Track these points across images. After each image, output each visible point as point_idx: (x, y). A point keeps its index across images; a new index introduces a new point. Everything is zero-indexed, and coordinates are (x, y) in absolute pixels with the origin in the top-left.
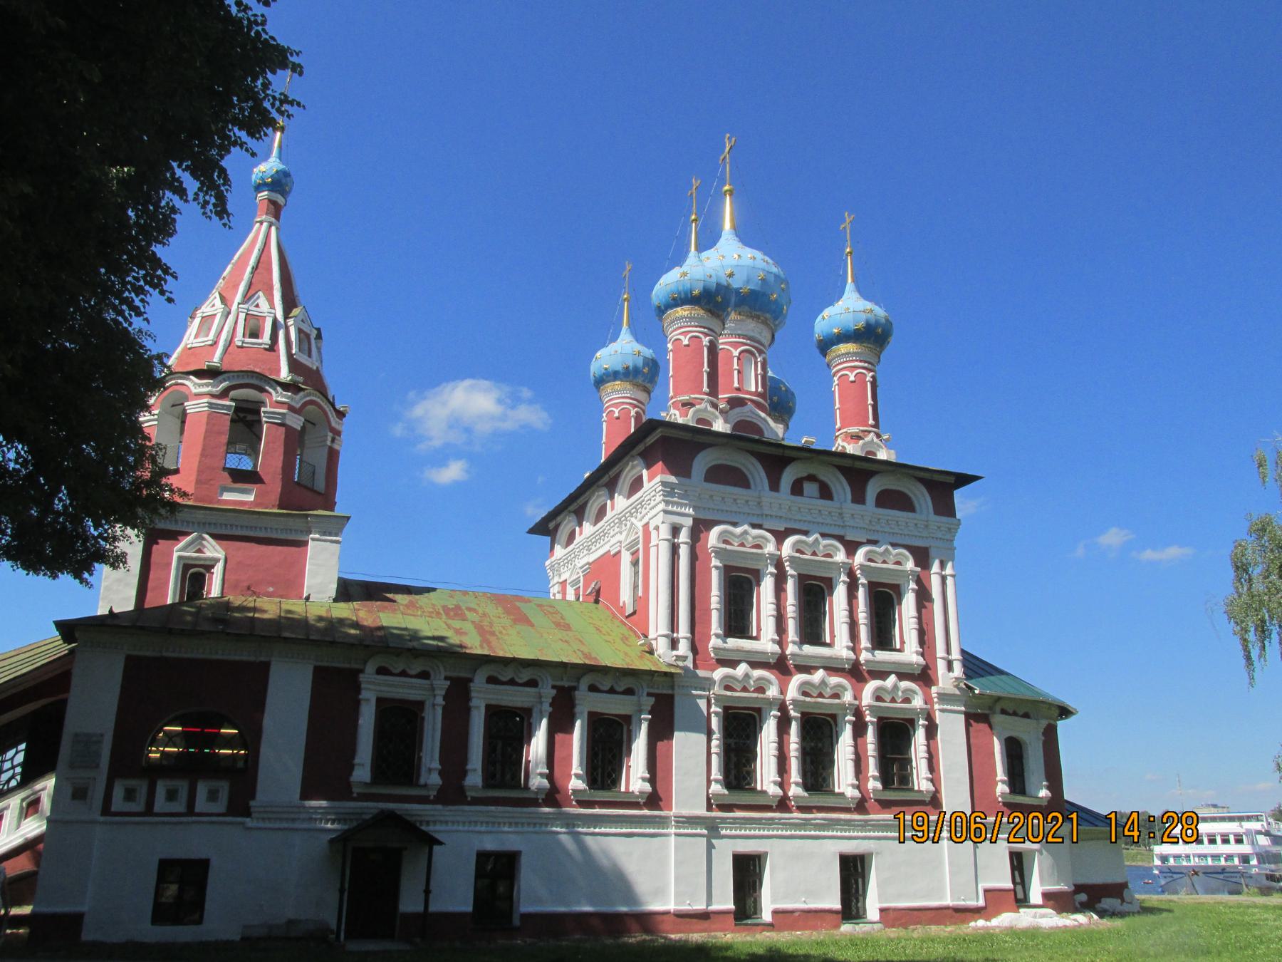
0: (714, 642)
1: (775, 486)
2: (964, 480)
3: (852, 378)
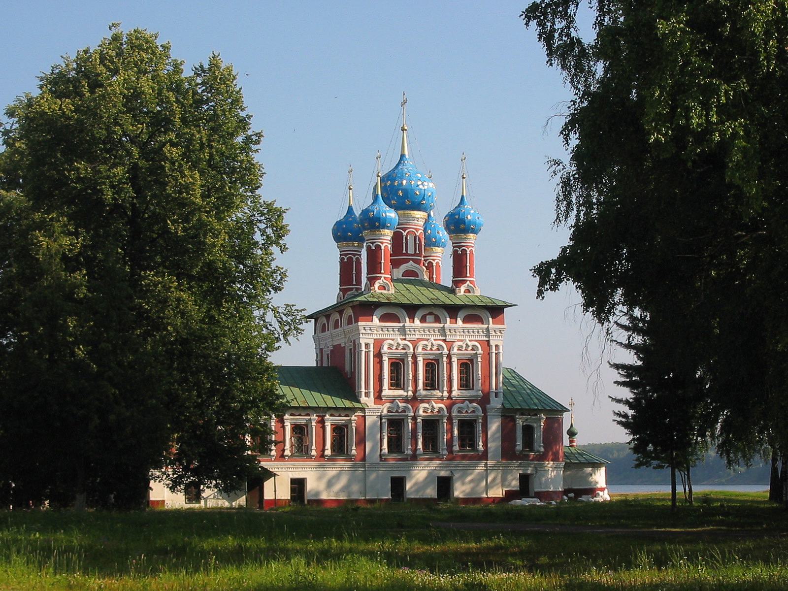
0: (384, 393)
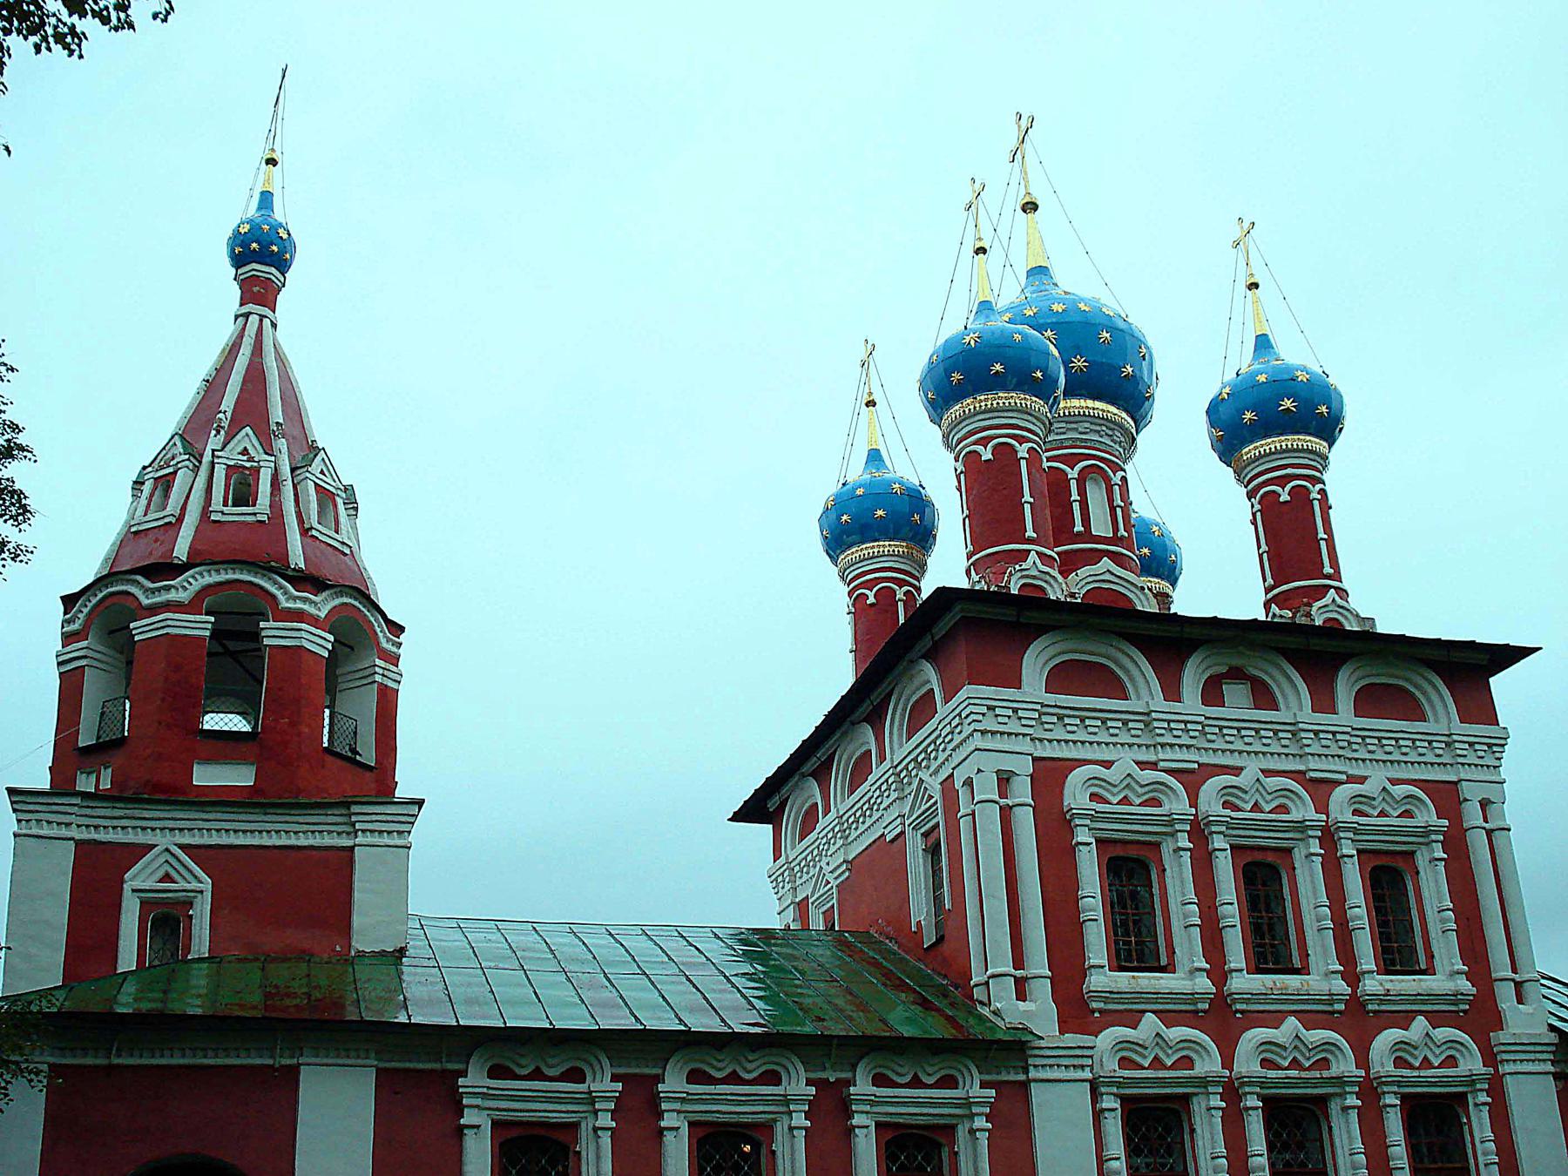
1: (1172, 691)
2: (1507, 656)
3: (1285, 497)
